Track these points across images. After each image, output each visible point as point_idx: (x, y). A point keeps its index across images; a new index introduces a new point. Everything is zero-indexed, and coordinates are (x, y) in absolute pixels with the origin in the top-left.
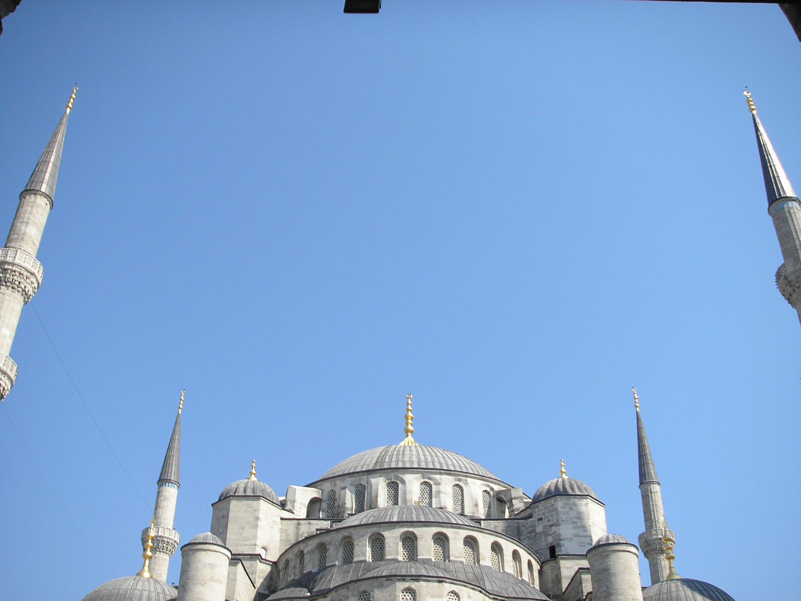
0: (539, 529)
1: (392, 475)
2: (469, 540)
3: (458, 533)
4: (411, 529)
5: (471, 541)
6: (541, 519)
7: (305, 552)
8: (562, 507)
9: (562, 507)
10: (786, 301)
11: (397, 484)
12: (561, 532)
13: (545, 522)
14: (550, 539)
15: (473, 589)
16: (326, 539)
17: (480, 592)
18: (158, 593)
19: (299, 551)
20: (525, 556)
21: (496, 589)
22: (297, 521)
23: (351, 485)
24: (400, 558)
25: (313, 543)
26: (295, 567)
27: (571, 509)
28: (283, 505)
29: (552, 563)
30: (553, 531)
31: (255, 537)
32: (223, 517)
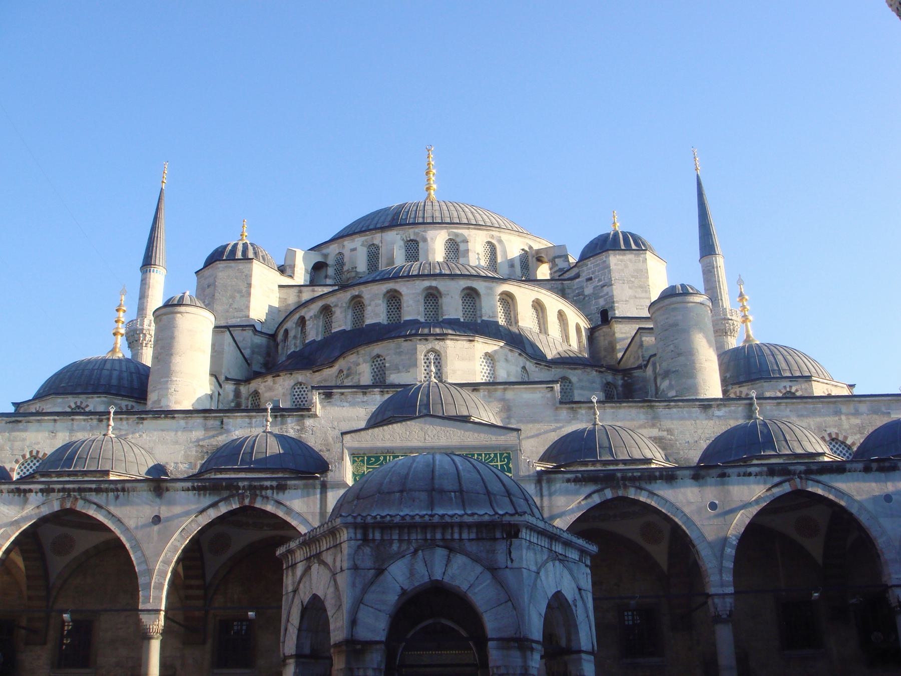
0: (588, 291)
1: (411, 231)
2: (504, 297)
3: (491, 289)
4: (434, 283)
5: (508, 299)
6: (591, 279)
7: (307, 318)
8: (615, 264)
9: (615, 264)
10: (894, 14)
11: (416, 242)
12: (615, 293)
13: (595, 282)
14: (601, 302)
15: (511, 350)
16: (331, 300)
17: (520, 354)
18: (131, 373)
22: (296, 290)
23: (362, 245)
24: (422, 320)
25: (316, 307)
26: (295, 337)
27: (626, 266)
28: (282, 270)
29: (605, 329)
30: (605, 292)
31: (248, 307)
32: (209, 286)
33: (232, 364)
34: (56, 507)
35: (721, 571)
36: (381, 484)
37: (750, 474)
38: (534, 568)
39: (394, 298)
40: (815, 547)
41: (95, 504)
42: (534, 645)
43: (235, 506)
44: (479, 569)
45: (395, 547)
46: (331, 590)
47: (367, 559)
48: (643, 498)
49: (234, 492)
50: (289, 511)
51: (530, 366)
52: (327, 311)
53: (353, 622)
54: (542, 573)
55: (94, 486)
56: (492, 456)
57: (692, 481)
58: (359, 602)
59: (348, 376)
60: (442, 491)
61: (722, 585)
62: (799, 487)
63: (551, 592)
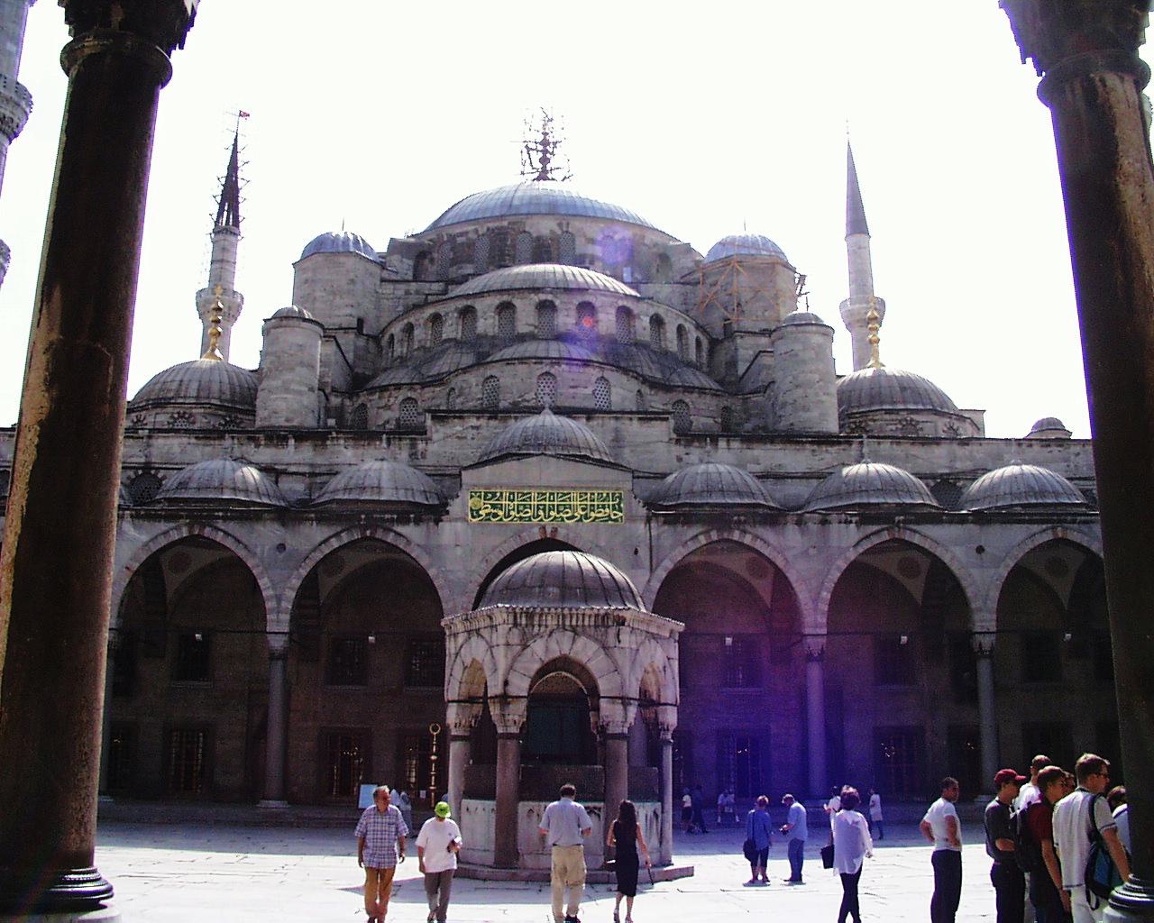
16: (441, 309)
19: (407, 325)
20: (693, 334)
21: (659, 376)
33: (336, 377)
34: (185, 532)
35: (816, 609)
36: (525, 580)
37: (851, 522)
38: (634, 646)
39: (506, 308)
40: (916, 587)
41: (221, 530)
42: (632, 701)
43: (357, 536)
44: (594, 646)
45: (536, 629)
46: (488, 657)
47: (515, 637)
48: (747, 540)
49: (357, 523)
50: (409, 542)
51: (646, 390)
52: (436, 319)
53: (506, 683)
54: (641, 649)
55: (221, 514)
56: (605, 495)
57: (796, 527)
58: (511, 668)
59: (459, 396)
60: (571, 588)
61: (816, 627)
62: (897, 536)
63: (647, 662)
